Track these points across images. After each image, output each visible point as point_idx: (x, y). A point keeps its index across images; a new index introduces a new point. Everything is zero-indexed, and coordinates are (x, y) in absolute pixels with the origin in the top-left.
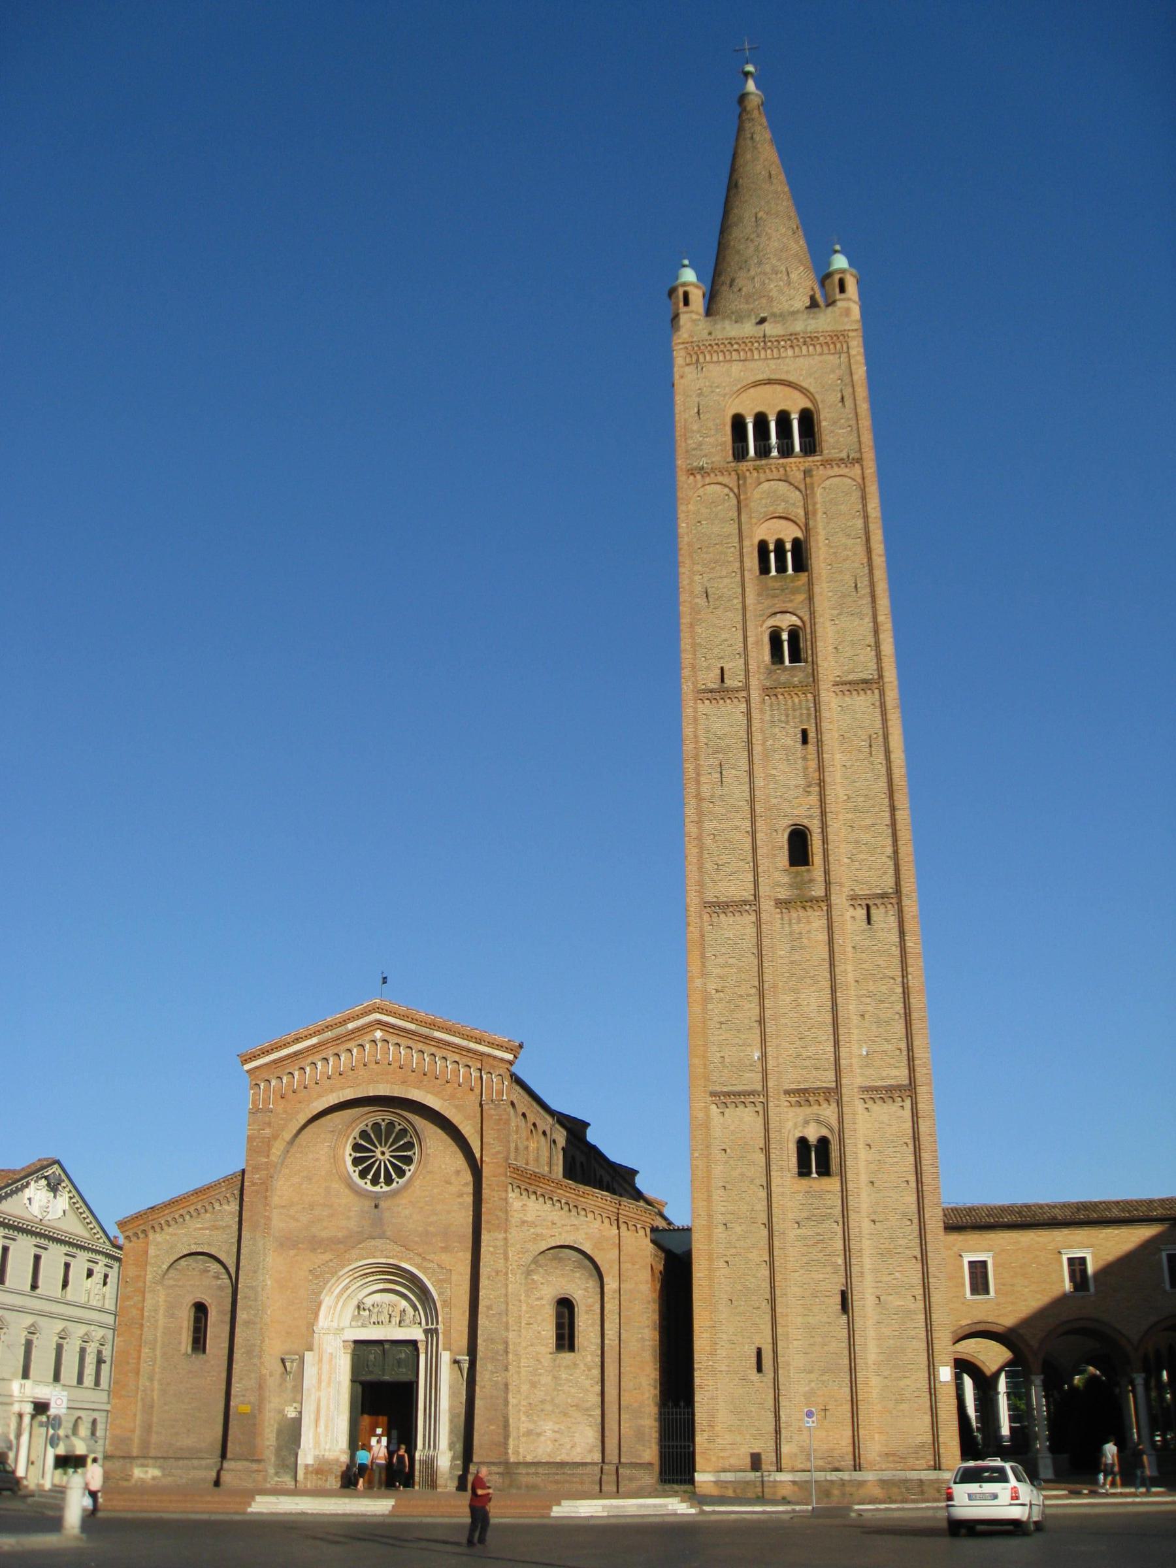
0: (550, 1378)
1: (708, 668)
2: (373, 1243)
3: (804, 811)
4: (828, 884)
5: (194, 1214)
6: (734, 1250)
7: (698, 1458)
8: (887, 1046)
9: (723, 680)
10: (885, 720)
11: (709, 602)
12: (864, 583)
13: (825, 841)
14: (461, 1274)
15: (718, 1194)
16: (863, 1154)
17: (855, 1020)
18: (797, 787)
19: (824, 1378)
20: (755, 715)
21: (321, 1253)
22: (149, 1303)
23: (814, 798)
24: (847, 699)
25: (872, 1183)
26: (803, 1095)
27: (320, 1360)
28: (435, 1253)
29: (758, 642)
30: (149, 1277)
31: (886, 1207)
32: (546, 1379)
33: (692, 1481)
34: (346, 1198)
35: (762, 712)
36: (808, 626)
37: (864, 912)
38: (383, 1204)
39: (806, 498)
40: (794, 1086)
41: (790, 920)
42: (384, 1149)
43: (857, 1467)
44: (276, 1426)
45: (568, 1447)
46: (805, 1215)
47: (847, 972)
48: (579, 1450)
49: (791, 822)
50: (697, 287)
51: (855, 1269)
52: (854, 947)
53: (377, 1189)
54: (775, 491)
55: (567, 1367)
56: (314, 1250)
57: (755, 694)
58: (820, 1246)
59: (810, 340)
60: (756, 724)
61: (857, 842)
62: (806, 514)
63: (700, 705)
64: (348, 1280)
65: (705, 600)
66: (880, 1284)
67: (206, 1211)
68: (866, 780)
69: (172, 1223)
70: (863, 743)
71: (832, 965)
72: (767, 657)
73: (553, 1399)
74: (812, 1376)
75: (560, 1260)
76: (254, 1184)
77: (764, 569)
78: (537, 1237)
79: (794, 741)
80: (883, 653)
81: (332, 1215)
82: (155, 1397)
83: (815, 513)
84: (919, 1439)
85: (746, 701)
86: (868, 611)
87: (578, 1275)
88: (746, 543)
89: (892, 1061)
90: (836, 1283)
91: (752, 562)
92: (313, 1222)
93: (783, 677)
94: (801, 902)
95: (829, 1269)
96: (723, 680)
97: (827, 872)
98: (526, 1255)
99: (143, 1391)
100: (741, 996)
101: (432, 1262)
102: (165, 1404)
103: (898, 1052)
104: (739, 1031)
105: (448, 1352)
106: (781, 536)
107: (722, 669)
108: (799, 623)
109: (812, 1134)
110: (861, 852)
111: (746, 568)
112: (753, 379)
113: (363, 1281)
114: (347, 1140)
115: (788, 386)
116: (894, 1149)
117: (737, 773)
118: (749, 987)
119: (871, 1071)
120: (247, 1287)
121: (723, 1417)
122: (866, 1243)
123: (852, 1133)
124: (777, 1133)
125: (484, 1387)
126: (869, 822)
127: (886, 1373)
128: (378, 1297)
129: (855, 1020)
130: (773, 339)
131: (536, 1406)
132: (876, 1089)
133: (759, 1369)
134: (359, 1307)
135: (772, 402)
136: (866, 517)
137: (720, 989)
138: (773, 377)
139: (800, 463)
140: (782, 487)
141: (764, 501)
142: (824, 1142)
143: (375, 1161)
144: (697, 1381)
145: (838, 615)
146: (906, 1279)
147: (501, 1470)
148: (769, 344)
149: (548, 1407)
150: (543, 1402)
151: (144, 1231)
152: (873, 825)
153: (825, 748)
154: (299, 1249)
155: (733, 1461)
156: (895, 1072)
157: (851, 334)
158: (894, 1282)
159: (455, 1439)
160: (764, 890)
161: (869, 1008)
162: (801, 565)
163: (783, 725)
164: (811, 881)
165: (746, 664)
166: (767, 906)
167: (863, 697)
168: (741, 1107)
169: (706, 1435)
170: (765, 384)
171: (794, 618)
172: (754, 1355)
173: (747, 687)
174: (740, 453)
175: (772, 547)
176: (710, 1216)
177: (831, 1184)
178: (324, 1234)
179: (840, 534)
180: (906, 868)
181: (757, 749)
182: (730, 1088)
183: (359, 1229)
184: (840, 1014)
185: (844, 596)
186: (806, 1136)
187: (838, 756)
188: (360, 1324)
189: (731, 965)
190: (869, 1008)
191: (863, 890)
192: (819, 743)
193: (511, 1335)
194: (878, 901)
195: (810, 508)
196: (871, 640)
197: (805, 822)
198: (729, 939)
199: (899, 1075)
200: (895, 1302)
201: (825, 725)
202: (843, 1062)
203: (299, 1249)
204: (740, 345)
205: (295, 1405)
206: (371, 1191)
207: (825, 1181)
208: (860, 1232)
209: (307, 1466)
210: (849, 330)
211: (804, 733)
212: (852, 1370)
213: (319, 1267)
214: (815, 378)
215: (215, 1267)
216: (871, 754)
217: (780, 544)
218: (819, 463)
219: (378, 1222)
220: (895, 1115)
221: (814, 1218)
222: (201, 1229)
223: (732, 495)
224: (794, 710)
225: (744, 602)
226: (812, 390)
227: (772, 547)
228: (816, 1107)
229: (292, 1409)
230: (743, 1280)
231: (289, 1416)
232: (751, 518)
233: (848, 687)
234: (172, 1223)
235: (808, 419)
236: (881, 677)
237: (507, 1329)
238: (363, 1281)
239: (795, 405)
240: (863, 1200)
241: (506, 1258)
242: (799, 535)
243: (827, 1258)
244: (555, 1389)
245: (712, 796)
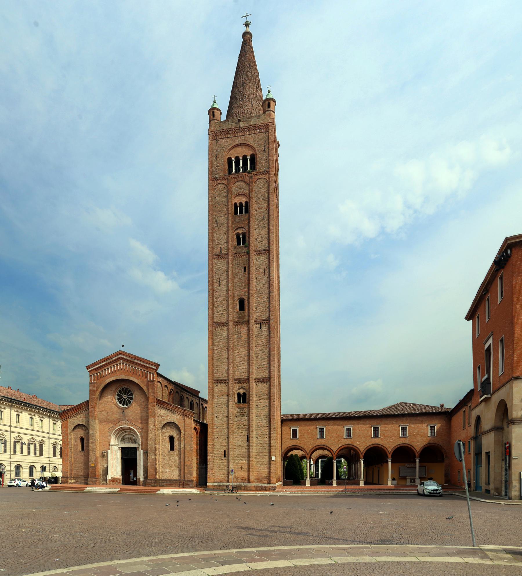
0: (168, 457)
1: (217, 248)
2: (123, 421)
3: (243, 294)
4: (249, 316)
5: (78, 414)
6: (219, 424)
7: (208, 479)
8: (264, 366)
9: (221, 252)
11: (217, 225)
12: (266, 216)
13: (249, 303)
14: (146, 430)
15: (215, 408)
16: (255, 398)
17: (255, 358)
18: (242, 286)
19: (241, 459)
20: (230, 263)
22: (69, 438)
23: (246, 289)
24: (258, 256)
25: (257, 405)
26: (239, 381)
27: (112, 452)
29: (232, 238)
30: (69, 431)
31: (261, 412)
32: (167, 458)
33: (206, 485)
34: (115, 409)
35: (232, 261)
37: (260, 325)
38: (125, 411)
39: (249, 186)
40: (237, 378)
41: (238, 328)
42: (125, 396)
43: (249, 482)
44: (102, 469)
45: (172, 476)
46: (239, 414)
47: (253, 343)
48: (175, 476)
49: (239, 297)
51: (251, 429)
52: (256, 336)
53: (124, 406)
54: (240, 185)
55: (172, 455)
56: (109, 423)
58: (242, 423)
59: (256, 127)
60: (230, 266)
61: (259, 303)
63: (214, 260)
64: (118, 431)
66: (258, 434)
67: (81, 413)
68: (263, 283)
69: (73, 416)
70: (263, 271)
71: (249, 341)
72: (236, 243)
73: (169, 463)
74: (238, 458)
75: (170, 426)
76: (91, 405)
77: (236, 213)
78: (164, 420)
79: (241, 270)
80: (270, 240)
81: (112, 414)
82: (73, 462)
83: (252, 191)
84: (265, 476)
86: (266, 226)
87: (175, 430)
88: (230, 204)
89: (265, 371)
90: (245, 434)
91: (232, 210)
92: (108, 416)
93: (240, 250)
94: (241, 322)
95: (244, 429)
97: (249, 313)
98: (161, 424)
99: (70, 460)
100: (223, 351)
102: (76, 464)
103: (266, 368)
104: (222, 361)
105: (142, 451)
106: (241, 201)
107: (221, 247)
108: (245, 231)
109: (241, 391)
110: (260, 306)
111: (229, 213)
112: (235, 144)
113: (122, 432)
114: (116, 393)
115: (247, 146)
116: (263, 396)
117: (224, 282)
118: (225, 349)
119: (259, 373)
120: (92, 433)
121: (215, 469)
122: (254, 422)
123: (252, 392)
124: (232, 392)
125: (150, 460)
126: (262, 297)
127: (258, 458)
128: (127, 436)
129: (255, 358)
130: (243, 128)
131: (164, 465)
132: (260, 379)
133: (225, 456)
134: (122, 438)
135: (241, 152)
137: (217, 349)
138: (242, 142)
140: (242, 184)
141: (236, 189)
142: (244, 394)
143: (123, 399)
144: (208, 459)
145: (258, 228)
146: (265, 433)
147: (154, 481)
148: (241, 130)
149: (168, 465)
150: (166, 464)
151: (66, 419)
152: (264, 298)
153: (250, 273)
155: (217, 480)
156: (265, 374)
158: (262, 433)
160: (230, 318)
161: (259, 355)
162: (247, 211)
163: (239, 266)
164: (245, 316)
166: (231, 323)
167: (263, 256)
168: (222, 384)
169: (210, 473)
170: (239, 146)
171: (244, 230)
172: (224, 452)
173: (228, 254)
175: (238, 205)
176: (213, 414)
177: (245, 405)
178: (111, 419)
179: (260, 199)
180: (272, 311)
181: (230, 273)
182: (219, 378)
183: (120, 418)
184: (250, 356)
185: (260, 221)
186: (240, 392)
187: (254, 276)
189: (221, 342)
190: (259, 355)
191: (259, 318)
192: (249, 271)
193: (157, 446)
194: (264, 322)
195: (251, 190)
196: (267, 236)
197: (244, 297)
198: (220, 334)
199: (265, 374)
200: (261, 439)
201: (251, 265)
202: (250, 371)
206: (122, 407)
207: (244, 404)
208: (253, 419)
209: (109, 479)
210: (269, 123)
211: (245, 268)
212: (249, 457)
214: (256, 142)
215: (84, 428)
216: (264, 274)
217: (241, 203)
219: (124, 416)
220: (264, 387)
221: (241, 415)
222: (80, 418)
224: (242, 260)
225: (228, 225)
226: (255, 146)
227: (238, 205)
228: (242, 384)
229: (105, 465)
230: (221, 432)
232: (231, 195)
233: (259, 252)
234: (73, 416)
235: (253, 158)
236: (269, 248)
237: (156, 444)
238: (122, 432)
239: (248, 153)
240: (254, 410)
241: (155, 425)
242: (248, 200)
243: (244, 426)
244: (169, 461)
245: (217, 289)
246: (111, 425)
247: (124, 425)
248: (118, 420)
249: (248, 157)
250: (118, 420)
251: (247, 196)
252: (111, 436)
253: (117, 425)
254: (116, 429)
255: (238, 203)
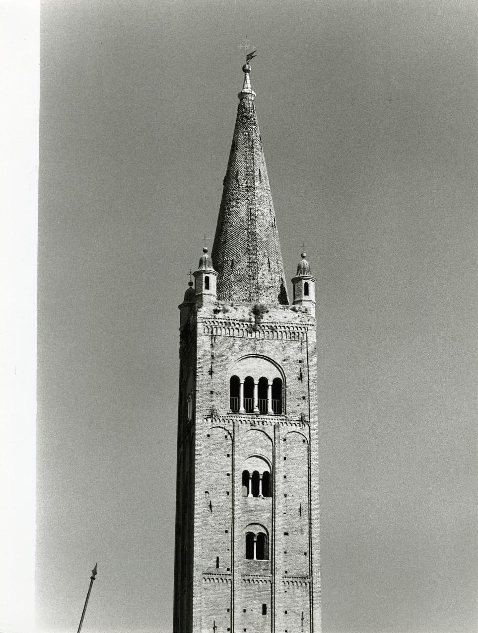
10: (312, 605)
12: (305, 507)
36: (270, 535)
50: (214, 274)
57: (237, 577)
62: (274, 456)
65: (209, 509)
72: (244, 552)
85: (231, 582)
96: (218, 567)
107: (218, 558)
108: (265, 533)
136: (309, 463)
139: (272, 419)
157: (310, 327)
162: (269, 491)
165: (233, 557)
170: (253, 357)
174: (235, 409)
192: (273, 615)
204: (240, 326)
211: (264, 606)
218: (283, 422)
223: (229, 437)
233: (291, 579)
235: (278, 384)
239: (271, 374)
242: (269, 471)
249: (270, 383)
251: (270, 463)
255: (251, 472)
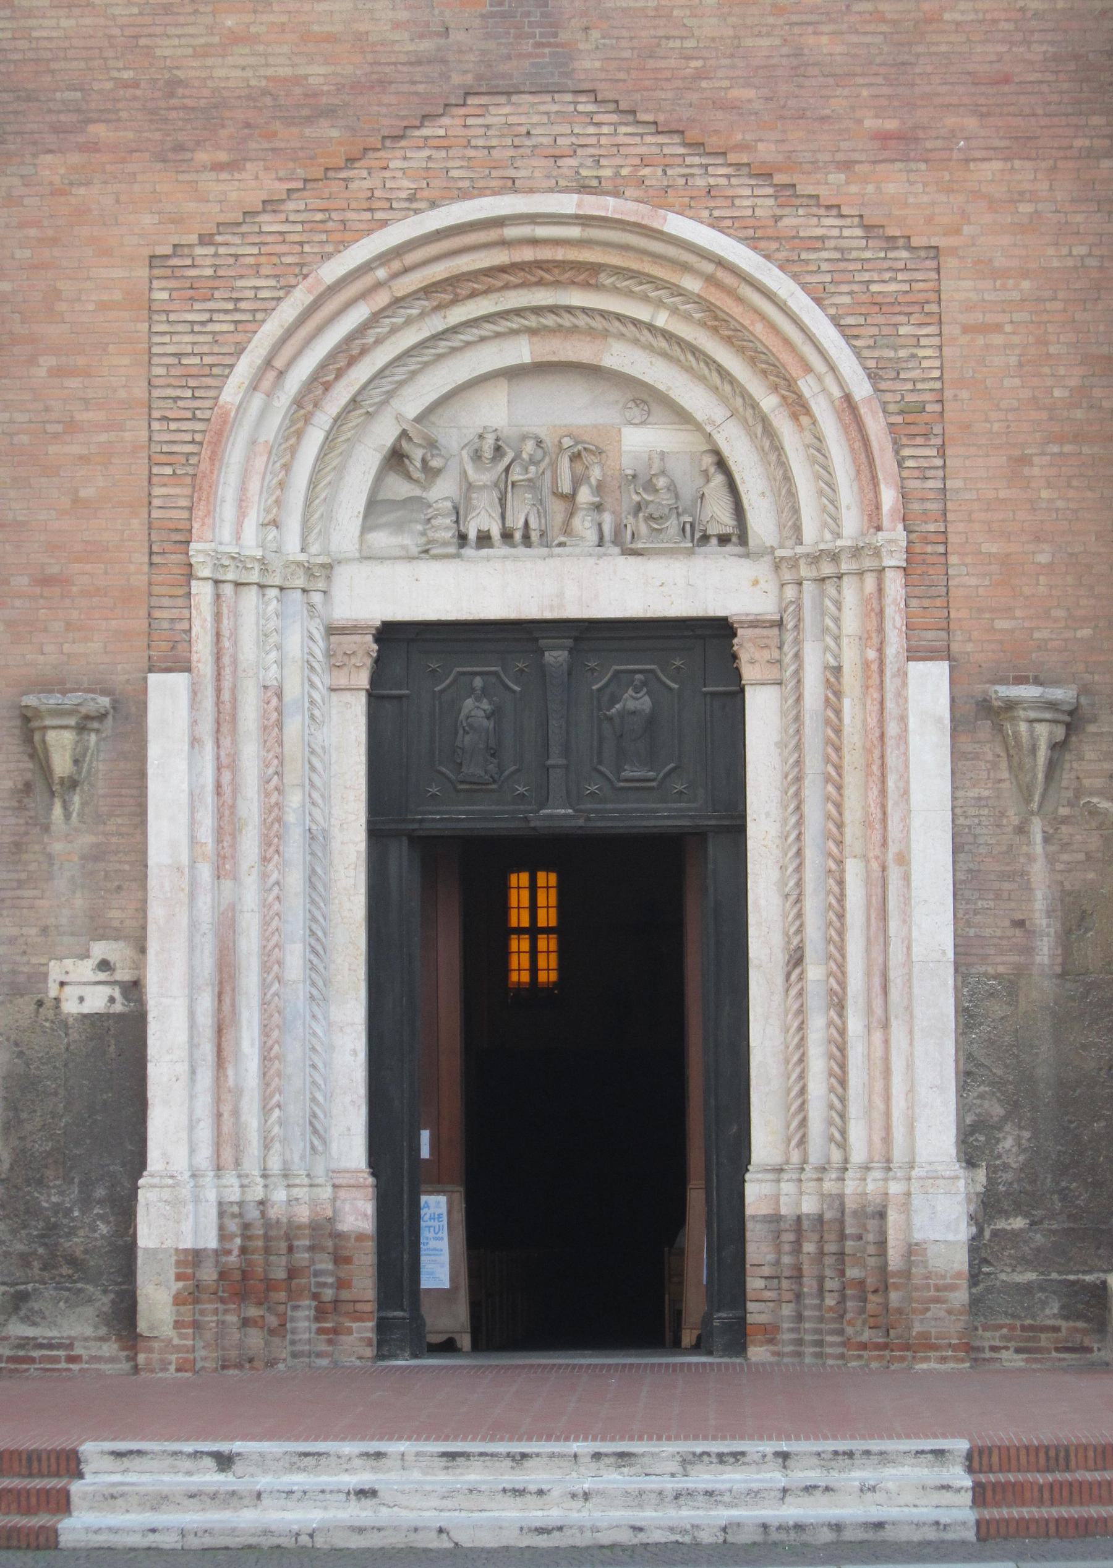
2: (500, 113)
21: (218, 167)
28: (846, 166)
101: (835, 208)
105: (942, 669)
134: (396, 458)
154: (92, 147)
159: (998, 1111)
188: (414, 550)
203: (92, 147)
205: (100, 950)
213: (205, 240)
229: (85, 970)
231: (71, 1007)
238: (437, 323)
246: (211, 183)
247: (512, 186)
248: (383, 84)
250: (383, 84)
252: (231, 393)
253: (362, 181)
254: (331, 271)
